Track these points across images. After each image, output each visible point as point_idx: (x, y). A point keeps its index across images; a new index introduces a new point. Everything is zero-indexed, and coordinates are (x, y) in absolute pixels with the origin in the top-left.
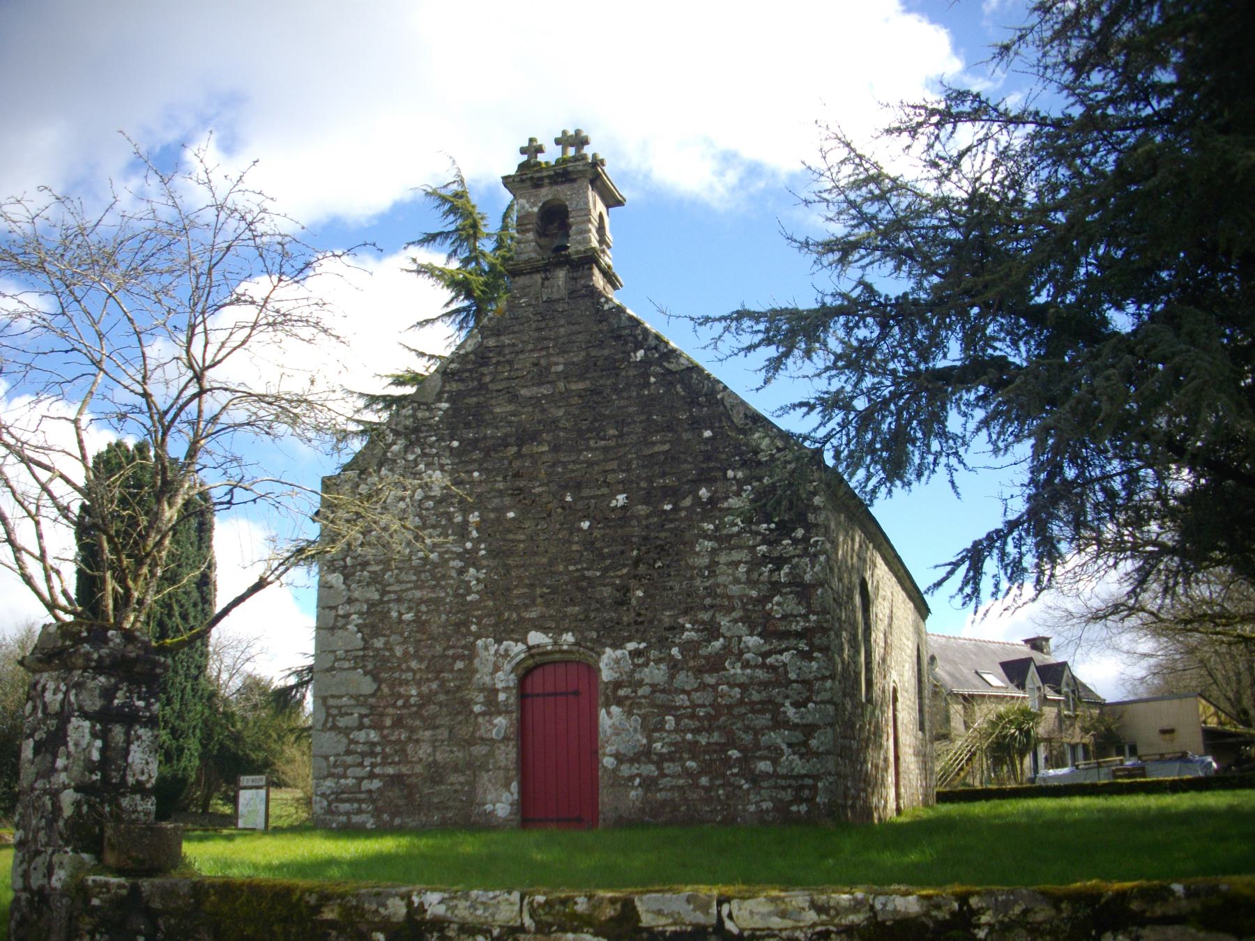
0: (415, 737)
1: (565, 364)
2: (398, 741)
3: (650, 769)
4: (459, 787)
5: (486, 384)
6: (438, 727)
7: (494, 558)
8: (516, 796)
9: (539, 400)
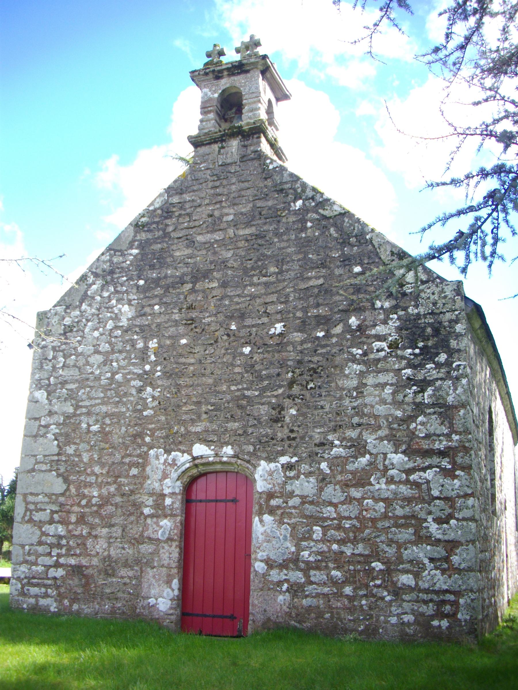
0: (94, 533)
1: (235, 215)
2: (81, 536)
3: (297, 576)
4: (127, 580)
5: (169, 233)
6: (113, 526)
7: (168, 378)
8: (176, 592)
9: (212, 244)
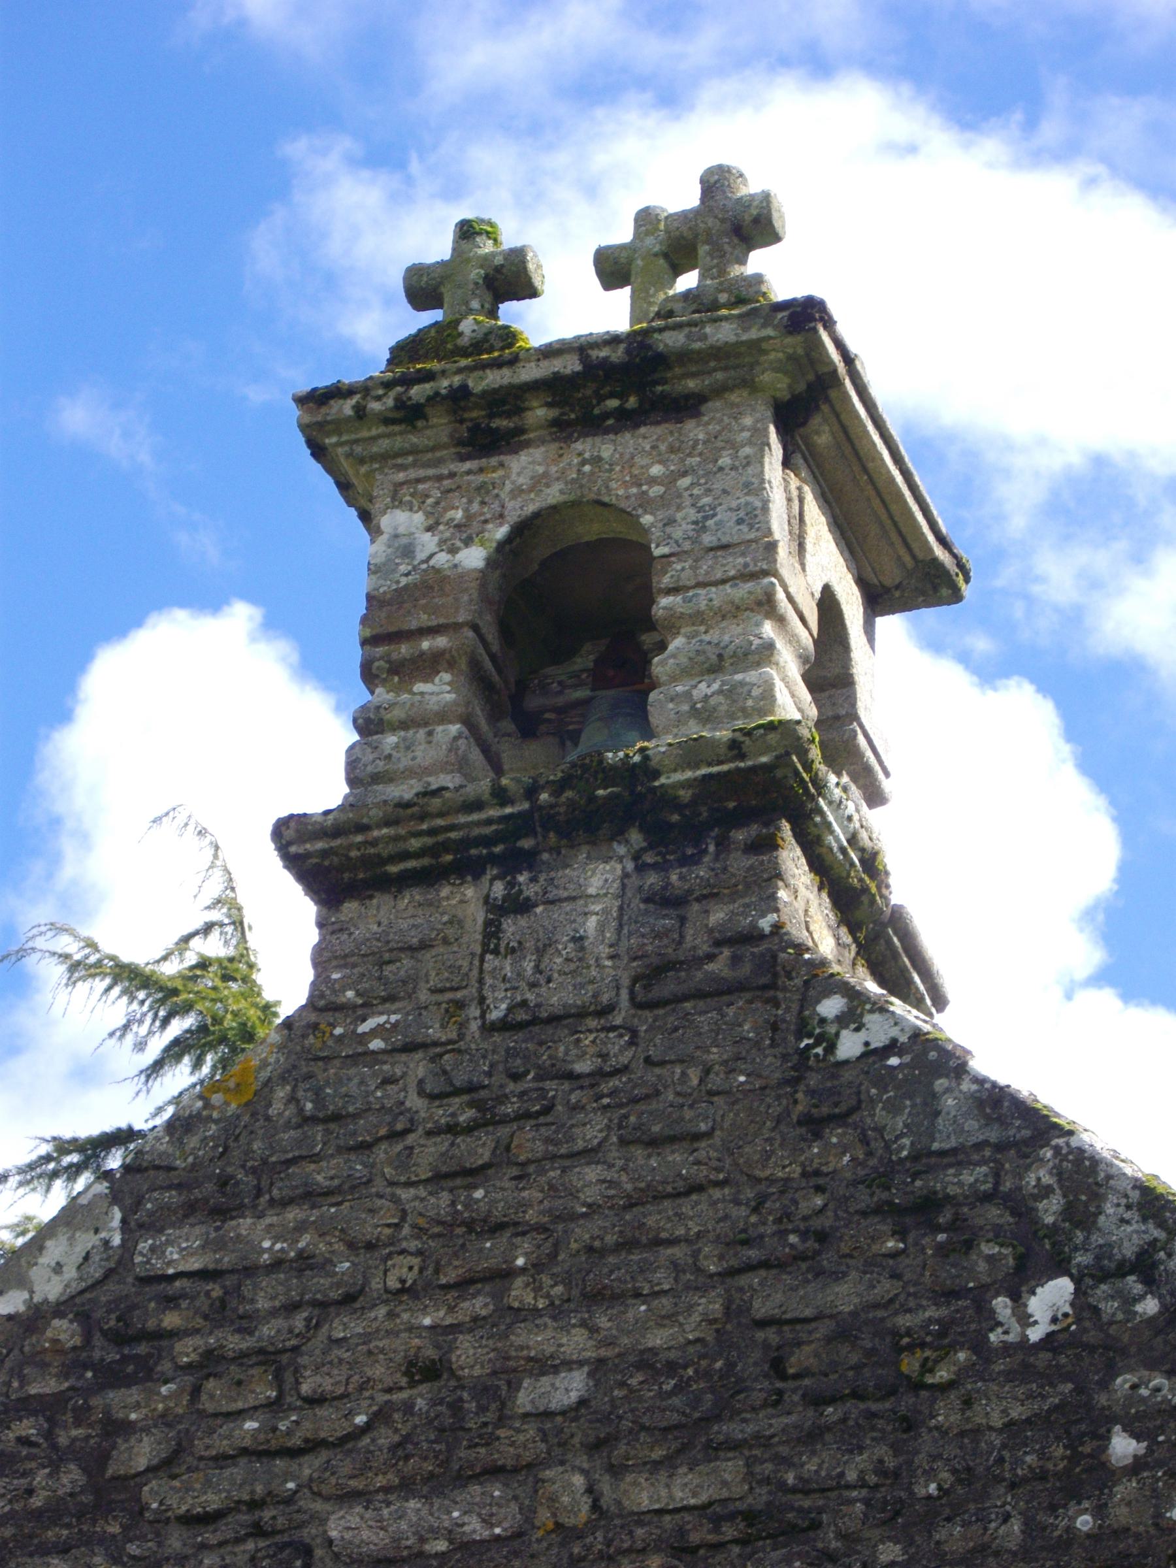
1: (598, 1368)
5: (132, 1482)
